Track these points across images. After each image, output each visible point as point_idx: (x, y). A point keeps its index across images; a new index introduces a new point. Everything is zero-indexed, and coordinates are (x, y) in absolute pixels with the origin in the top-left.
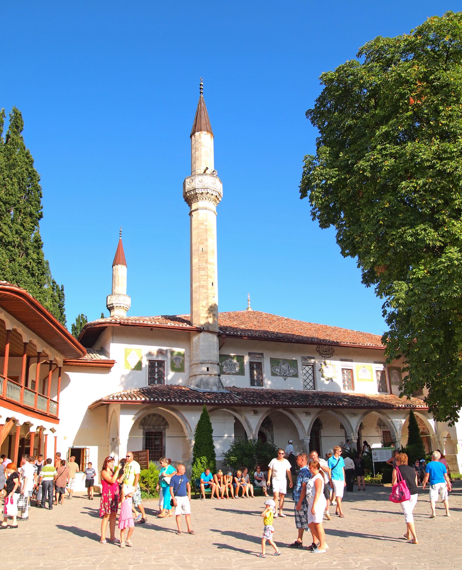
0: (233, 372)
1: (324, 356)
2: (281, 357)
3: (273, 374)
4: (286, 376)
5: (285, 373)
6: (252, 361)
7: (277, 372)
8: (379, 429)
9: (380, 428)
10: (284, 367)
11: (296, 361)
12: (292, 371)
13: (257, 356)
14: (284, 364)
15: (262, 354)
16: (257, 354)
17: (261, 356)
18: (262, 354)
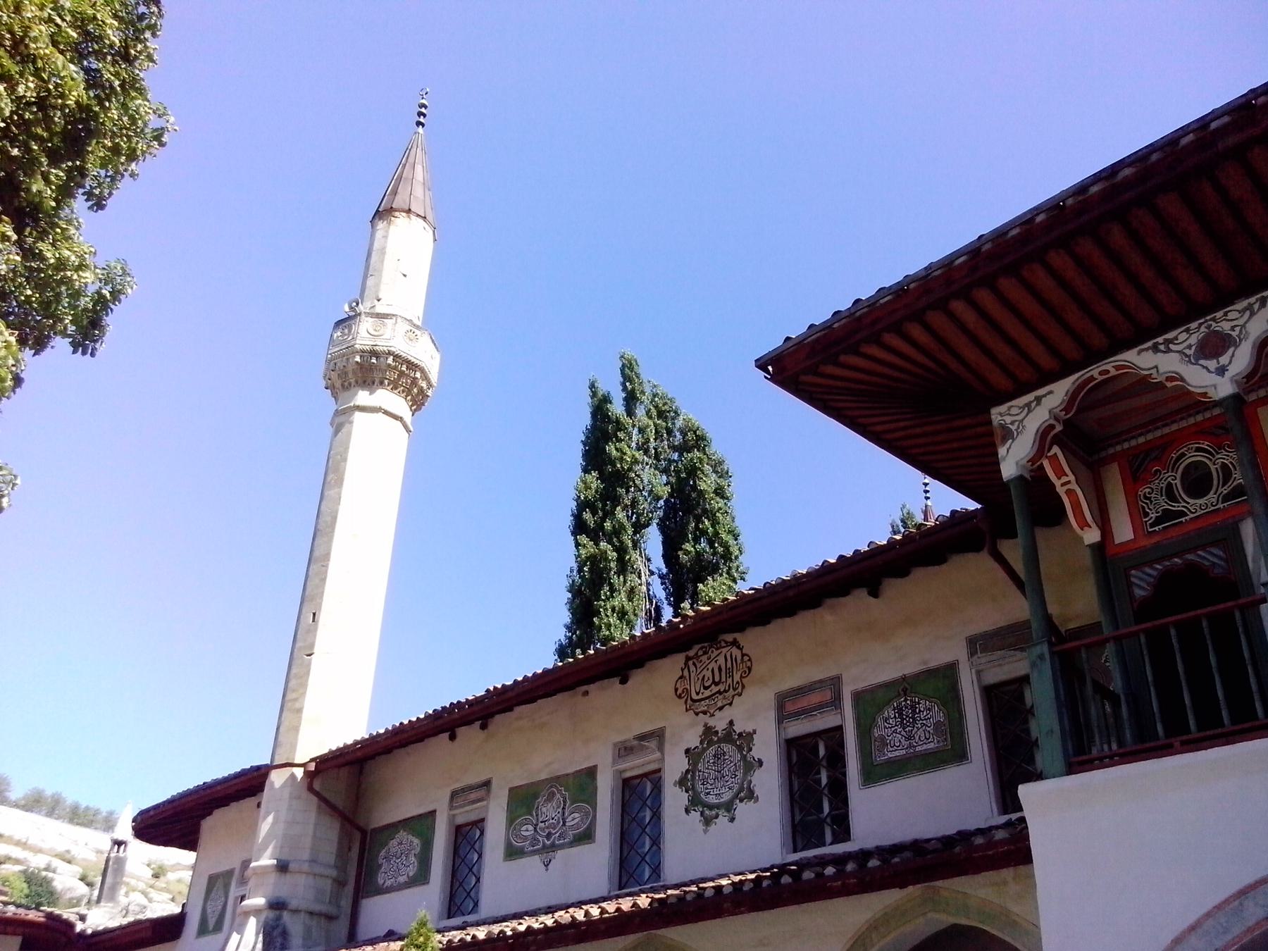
0: (402, 879)
1: (702, 706)
2: (543, 776)
3: (512, 853)
4: (554, 848)
5: (549, 836)
6: (460, 820)
7: (526, 838)
10: (549, 811)
11: (591, 772)
13: (473, 796)
15: (487, 784)
16: (471, 788)
17: (481, 793)
18: (487, 784)
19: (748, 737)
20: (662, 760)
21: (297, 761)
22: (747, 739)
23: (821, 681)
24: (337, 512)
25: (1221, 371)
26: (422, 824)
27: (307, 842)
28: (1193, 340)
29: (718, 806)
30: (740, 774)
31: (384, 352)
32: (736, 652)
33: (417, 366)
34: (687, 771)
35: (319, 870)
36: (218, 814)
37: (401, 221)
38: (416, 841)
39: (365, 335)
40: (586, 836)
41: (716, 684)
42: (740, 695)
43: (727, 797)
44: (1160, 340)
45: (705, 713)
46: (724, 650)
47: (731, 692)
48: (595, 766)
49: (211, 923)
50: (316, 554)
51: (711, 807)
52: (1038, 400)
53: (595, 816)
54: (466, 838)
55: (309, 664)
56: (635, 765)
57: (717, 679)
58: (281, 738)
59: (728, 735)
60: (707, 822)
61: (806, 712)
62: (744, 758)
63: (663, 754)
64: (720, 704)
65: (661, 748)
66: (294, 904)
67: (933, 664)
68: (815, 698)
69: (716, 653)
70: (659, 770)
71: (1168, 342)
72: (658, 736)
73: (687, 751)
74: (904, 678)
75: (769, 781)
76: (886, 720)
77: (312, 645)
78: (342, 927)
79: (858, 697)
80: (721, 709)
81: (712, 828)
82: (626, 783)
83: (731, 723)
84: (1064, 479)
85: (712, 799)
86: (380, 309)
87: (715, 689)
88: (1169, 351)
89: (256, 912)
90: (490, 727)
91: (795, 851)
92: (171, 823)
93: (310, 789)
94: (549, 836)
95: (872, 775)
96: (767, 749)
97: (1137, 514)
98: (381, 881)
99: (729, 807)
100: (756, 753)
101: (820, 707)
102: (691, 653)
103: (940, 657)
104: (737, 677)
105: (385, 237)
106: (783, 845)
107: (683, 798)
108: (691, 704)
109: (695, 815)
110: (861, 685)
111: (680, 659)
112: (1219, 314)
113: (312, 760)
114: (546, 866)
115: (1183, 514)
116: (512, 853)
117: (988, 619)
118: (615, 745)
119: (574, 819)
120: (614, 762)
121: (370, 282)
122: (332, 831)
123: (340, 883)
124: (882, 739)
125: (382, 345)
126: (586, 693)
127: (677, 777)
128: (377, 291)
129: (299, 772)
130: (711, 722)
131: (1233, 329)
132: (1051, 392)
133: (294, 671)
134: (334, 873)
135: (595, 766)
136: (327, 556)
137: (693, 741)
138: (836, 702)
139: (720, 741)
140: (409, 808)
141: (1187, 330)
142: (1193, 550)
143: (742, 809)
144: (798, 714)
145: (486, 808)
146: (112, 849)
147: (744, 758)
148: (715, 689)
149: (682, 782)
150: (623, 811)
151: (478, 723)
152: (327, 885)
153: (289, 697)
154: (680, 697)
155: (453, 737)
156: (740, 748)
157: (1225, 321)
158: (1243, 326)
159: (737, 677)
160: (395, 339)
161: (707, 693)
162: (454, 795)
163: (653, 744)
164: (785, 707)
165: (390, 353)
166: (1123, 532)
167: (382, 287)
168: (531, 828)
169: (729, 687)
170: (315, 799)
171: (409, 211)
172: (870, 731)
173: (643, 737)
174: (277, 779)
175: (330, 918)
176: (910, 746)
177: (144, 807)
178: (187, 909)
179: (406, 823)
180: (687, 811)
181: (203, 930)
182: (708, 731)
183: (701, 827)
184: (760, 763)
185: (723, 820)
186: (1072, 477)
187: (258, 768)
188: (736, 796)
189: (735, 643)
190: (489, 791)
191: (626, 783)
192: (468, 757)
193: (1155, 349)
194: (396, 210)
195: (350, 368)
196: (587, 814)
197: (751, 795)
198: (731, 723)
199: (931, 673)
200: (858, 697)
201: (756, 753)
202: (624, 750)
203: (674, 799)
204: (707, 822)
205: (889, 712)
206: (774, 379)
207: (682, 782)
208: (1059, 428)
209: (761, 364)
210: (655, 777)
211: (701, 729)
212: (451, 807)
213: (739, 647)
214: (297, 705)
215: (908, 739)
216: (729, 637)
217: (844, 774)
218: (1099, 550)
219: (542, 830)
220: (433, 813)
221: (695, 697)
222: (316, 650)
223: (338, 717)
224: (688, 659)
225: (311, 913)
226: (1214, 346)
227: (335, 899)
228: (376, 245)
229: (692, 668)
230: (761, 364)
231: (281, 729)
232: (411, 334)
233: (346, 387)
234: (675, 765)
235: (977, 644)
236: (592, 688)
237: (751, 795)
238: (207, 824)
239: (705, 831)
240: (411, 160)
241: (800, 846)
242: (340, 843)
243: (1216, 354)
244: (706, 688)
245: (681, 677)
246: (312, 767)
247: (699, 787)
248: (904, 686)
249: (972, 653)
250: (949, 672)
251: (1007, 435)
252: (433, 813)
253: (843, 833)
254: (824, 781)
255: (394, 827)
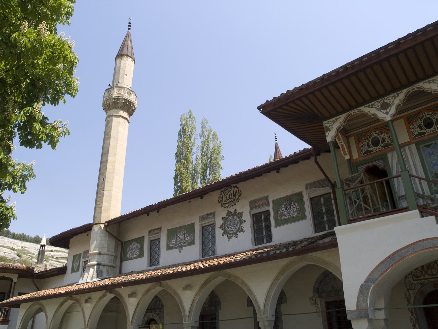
0: (135, 256)
1: (227, 205)
2: (178, 226)
4: (182, 246)
5: (180, 243)
6: (152, 239)
7: (173, 244)
8: (318, 300)
9: (320, 297)
10: (180, 236)
11: (193, 225)
12: (188, 238)
13: (156, 232)
14: (180, 232)
15: (160, 229)
17: (158, 231)
18: (160, 229)
19: (241, 214)
20: (215, 221)
21: (101, 222)
22: (240, 215)
23: (262, 198)
24: (109, 147)
25: (387, 113)
26: (140, 240)
27: (106, 245)
28: (379, 104)
29: (232, 234)
30: (239, 225)
31: (121, 99)
32: (236, 189)
33: (131, 103)
34: (223, 224)
35: (109, 253)
36: (75, 238)
37: (125, 58)
38: (139, 245)
39: (115, 93)
40: (192, 243)
41: (231, 199)
42: (238, 202)
43: (235, 231)
44: (370, 104)
45: (227, 207)
46: (233, 189)
47: (235, 201)
48: (194, 223)
49: (75, 269)
50: (103, 160)
51: (230, 234)
52: (336, 120)
53: (194, 237)
54: (154, 244)
55: (103, 194)
56: (206, 222)
57: (231, 197)
58: (96, 216)
59: (235, 214)
60: (229, 238)
61: (258, 207)
62: (240, 220)
63: (215, 219)
64: (232, 205)
65: (214, 217)
66: (103, 263)
67: (296, 192)
68: (261, 202)
69: (230, 190)
70: (214, 224)
71: (372, 105)
72: (213, 214)
73: (222, 218)
74: (287, 196)
75: (248, 226)
76: (282, 208)
77: (104, 188)
78: (117, 270)
79: (273, 202)
80: (232, 206)
81: (231, 240)
82: (203, 227)
83: (236, 210)
84: (340, 141)
85: (230, 232)
86: (119, 85)
87: (230, 200)
88: (372, 107)
89: (93, 266)
90: (160, 212)
91: (255, 245)
92: (61, 241)
93: (107, 231)
94: (180, 243)
95: (278, 224)
96: (247, 217)
97: (359, 151)
98: (128, 257)
99: (236, 234)
100: (243, 218)
101: (263, 205)
102: (223, 190)
103: (297, 190)
104: (237, 197)
105: (120, 63)
106: (252, 244)
107: (222, 232)
108: (223, 205)
109: (226, 237)
110: (274, 199)
111: (219, 191)
112: (386, 98)
113: (106, 222)
114: (180, 251)
115: (372, 151)
116: (169, 248)
117: (311, 179)
118: (200, 217)
119: (188, 238)
120: (200, 222)
121: (116, 77)
122: (113, 242)
123: (116, 257)
124: (281, 213)
125: (121, 96)
126: (190, 202)
127: (220, 226)
128: (118, 80)
129: (102, 226)
130: (230, 210)
131: (390, 102)
132: (340, 118)
133: (99, 196)
134: (114, 254)
135: (194, 223)
136: (107, 161)
137: (224, 215)
138: (267, 204)
139: (232, 215)
140: (135, 235)
141: (378, 102)
142: (375, 161)
143: (239, 234)
144: (256, 207)
145: (160, 235)
146: (41, 248)
147: (240, 220)
148: (230, 200)
149: (221, 227)
150: (203, 235)
151: (156, 211)
152: (113, 258)
153: (98, 203)
154: (219, 203)
155: (148, 215)
156: (239, 217)
157: (388, 99)
158: (393, 101)
159: (237, 197)
160: (124, 94)
161: (228, 201)
162: (150, 232)
163: (212, 216)
164: (252, 204)
165: (123, 99)
166: (356, 156)
167: (120, 78)
168: (174, 241)
169: (235, 200)
170: (108, 233)
171: (127, 55)
172: (277, 211)
173: (209, 214)
174: (96, 228)
175: (114, 267)
176: (289, 215)
177: (53, 236)
178: (67, 265)
179: (136, 240)
180: (223, 235)
181: (73, 271)
182: (229, 213)
183: (227, 239)
184: (245, 221)
185: (234, 237)
186: (342, 141)
187: (89, 224)
188: (238, 230)
189: (236, 187)
190: (161, 230)
191: (203, 227)
192: (154, 222)
193: (369, 106)
194: (124, 55)
195: (111, 104)
196: (192, 237)
197: (242, 230)
198: (236, 210)
199: (296, 194)
200: (273, 202)
201: (243, 218)
202: (202, 218)
203: (219, 232)
204: (229, 238)
205: (283, 206)
206: (262, 112)
207: (221, 227)
208: (342, 128)
209: (259, 108)
210: (213, 226)
211: (226, 212)
212: (149, 235)
213: (237, 188)
214: (100, 206)
215: (289, 213)
216: (234, 185)
217: (270, 224)
218: (349, 160)
219: (178, 241)
220: (144, 237)
221: (224, 202)
222: (105, 189)
223: (114, 209)
224: (222, 191)
225: (108, 266)
226: (385, 106)
227: (115, 261)
228: (117, 66)
229: (223, 194)
230: (259, 108)
231: (96, 213)
232: (129, 94)
233: (110, 109)
234: (219, 222)
235: (308, 186)
236: (192, 200)
237: (242, 230)
238: (71, 240)
239: (229, 241)
240: (127, 40)
241: (257, 244)
242: (115, 246)
243: (386, 109)
244: (227, 200)
245: (220, 197)
246: (106, 224)
247: (226, 228)
248: (288, 198)
249: (307, 189)
250: (300, 195)
251: (328, 130)
252: (143, 237)
253: (270, 239)
254: (264, 226)
255: (131, 241)
